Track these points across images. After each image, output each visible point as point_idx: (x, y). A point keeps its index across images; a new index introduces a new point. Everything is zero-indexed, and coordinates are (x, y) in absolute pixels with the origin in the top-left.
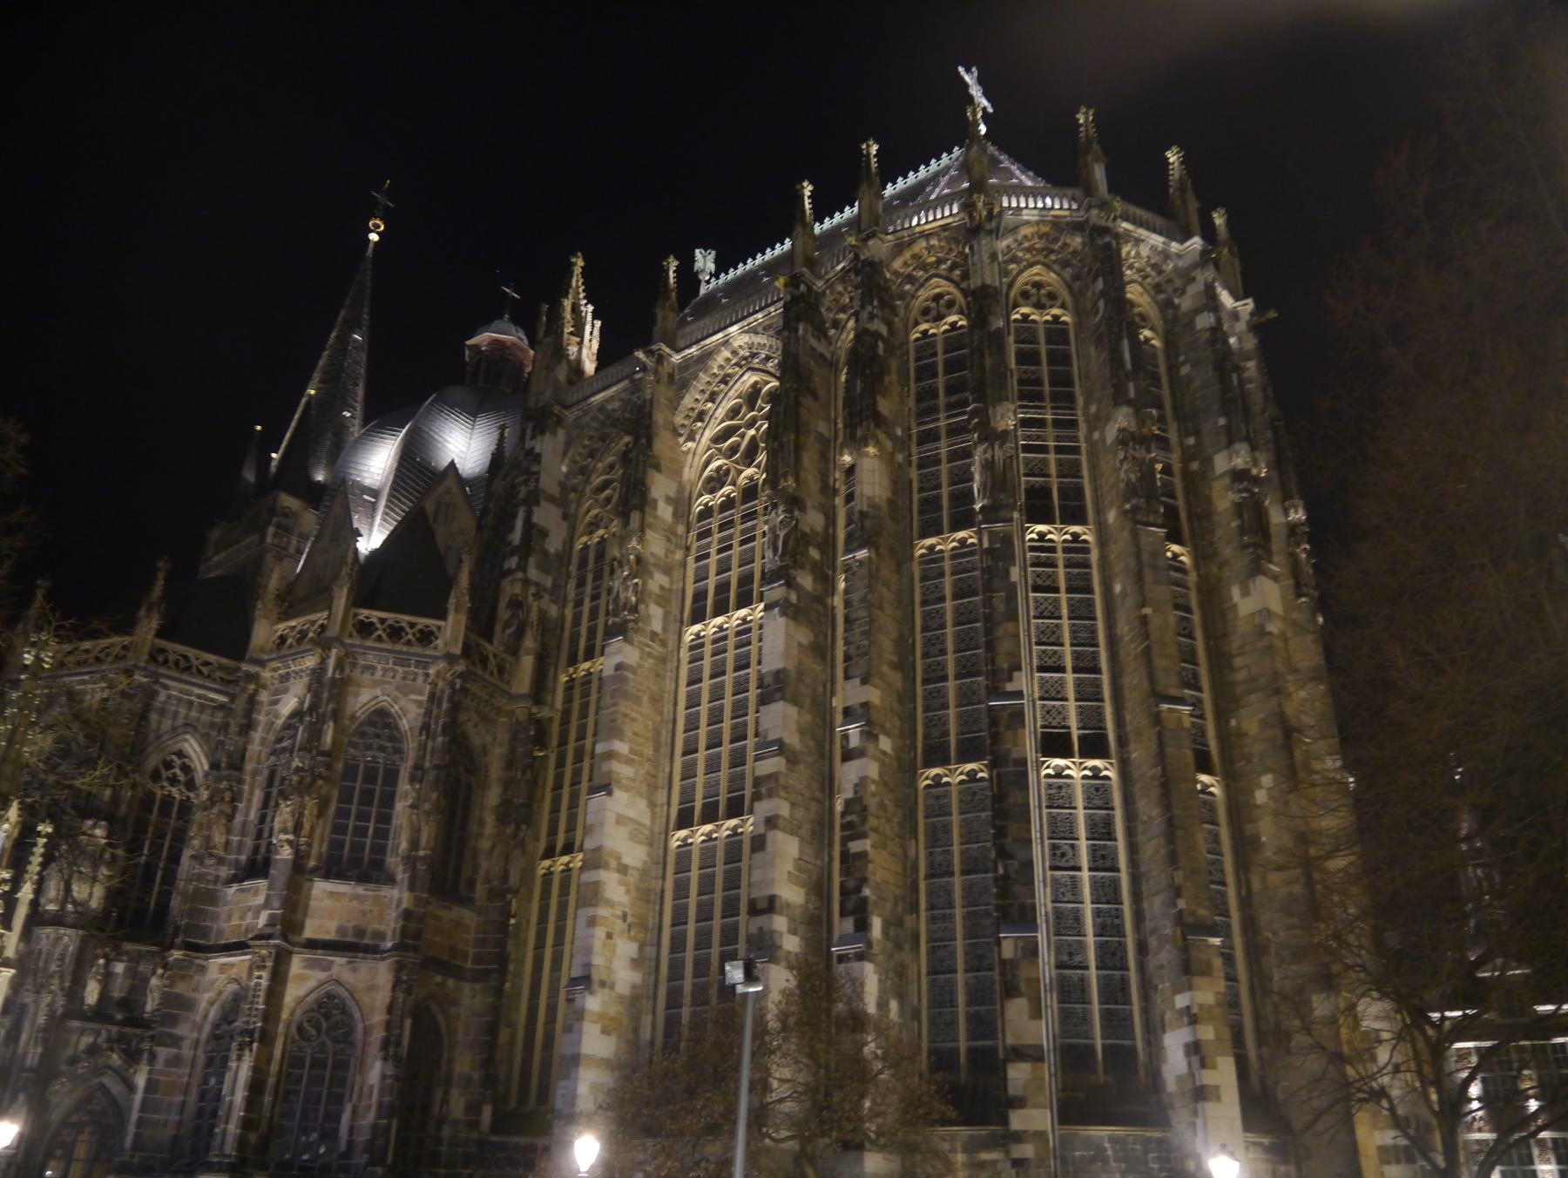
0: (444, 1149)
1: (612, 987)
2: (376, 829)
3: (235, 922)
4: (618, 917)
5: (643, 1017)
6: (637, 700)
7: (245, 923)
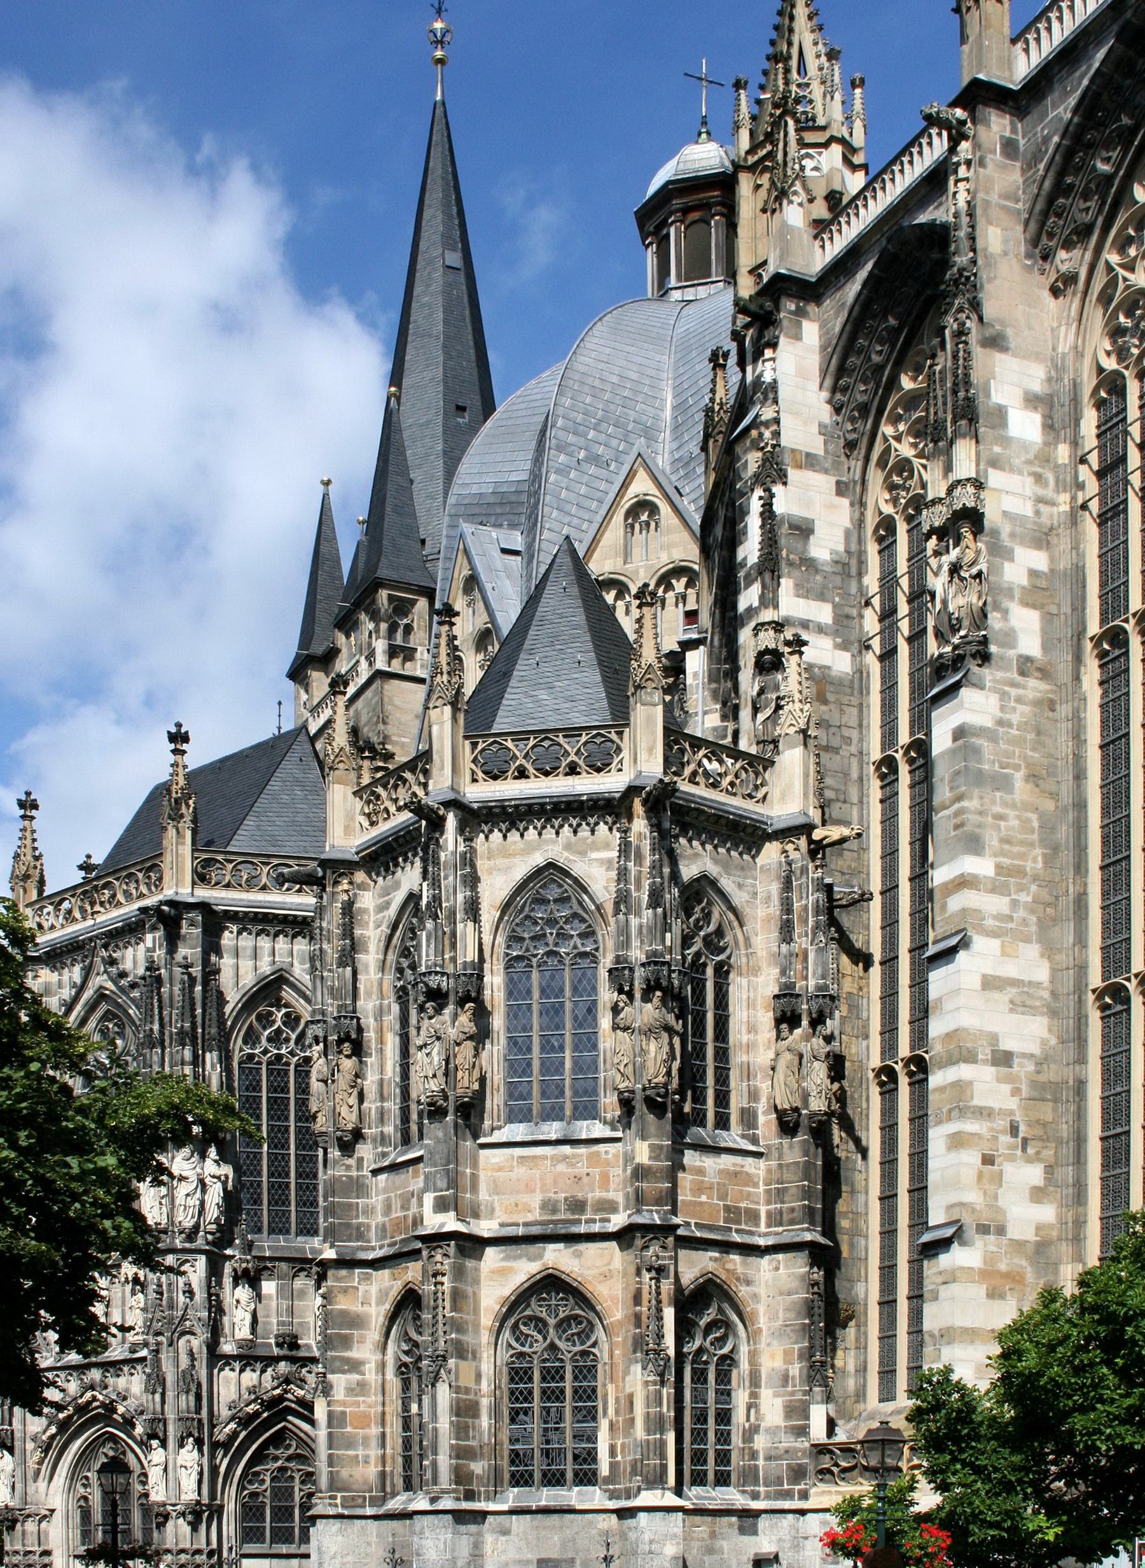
0: (761, 1462)
1: (1001, 1231)
2: (576, 1062)
3: (397, 1214)
4: (1003, 1132)
5: (1062, 1268)
6: (1003, 783)
7: (410, 1213)
